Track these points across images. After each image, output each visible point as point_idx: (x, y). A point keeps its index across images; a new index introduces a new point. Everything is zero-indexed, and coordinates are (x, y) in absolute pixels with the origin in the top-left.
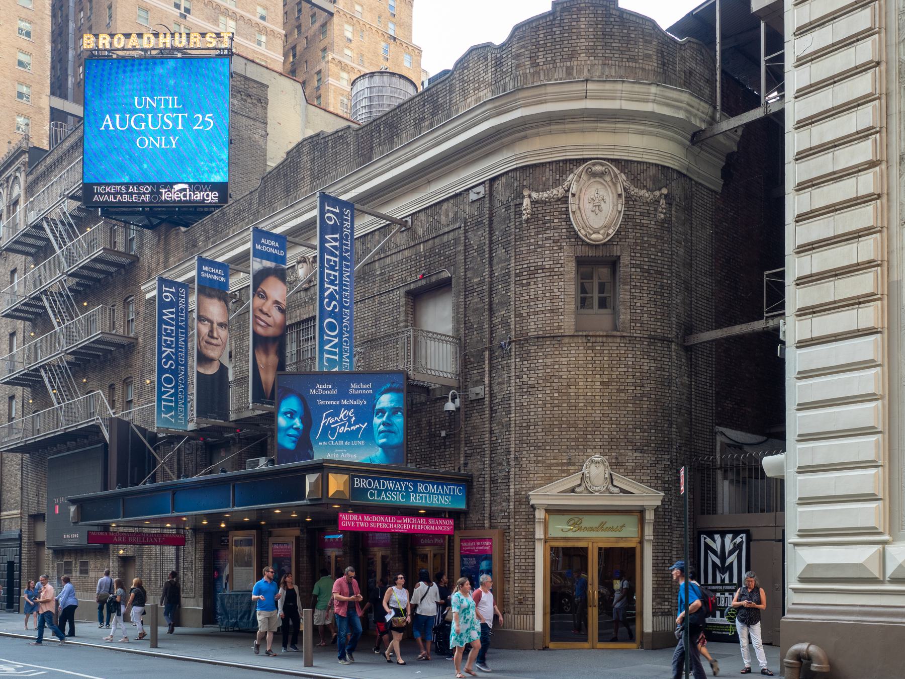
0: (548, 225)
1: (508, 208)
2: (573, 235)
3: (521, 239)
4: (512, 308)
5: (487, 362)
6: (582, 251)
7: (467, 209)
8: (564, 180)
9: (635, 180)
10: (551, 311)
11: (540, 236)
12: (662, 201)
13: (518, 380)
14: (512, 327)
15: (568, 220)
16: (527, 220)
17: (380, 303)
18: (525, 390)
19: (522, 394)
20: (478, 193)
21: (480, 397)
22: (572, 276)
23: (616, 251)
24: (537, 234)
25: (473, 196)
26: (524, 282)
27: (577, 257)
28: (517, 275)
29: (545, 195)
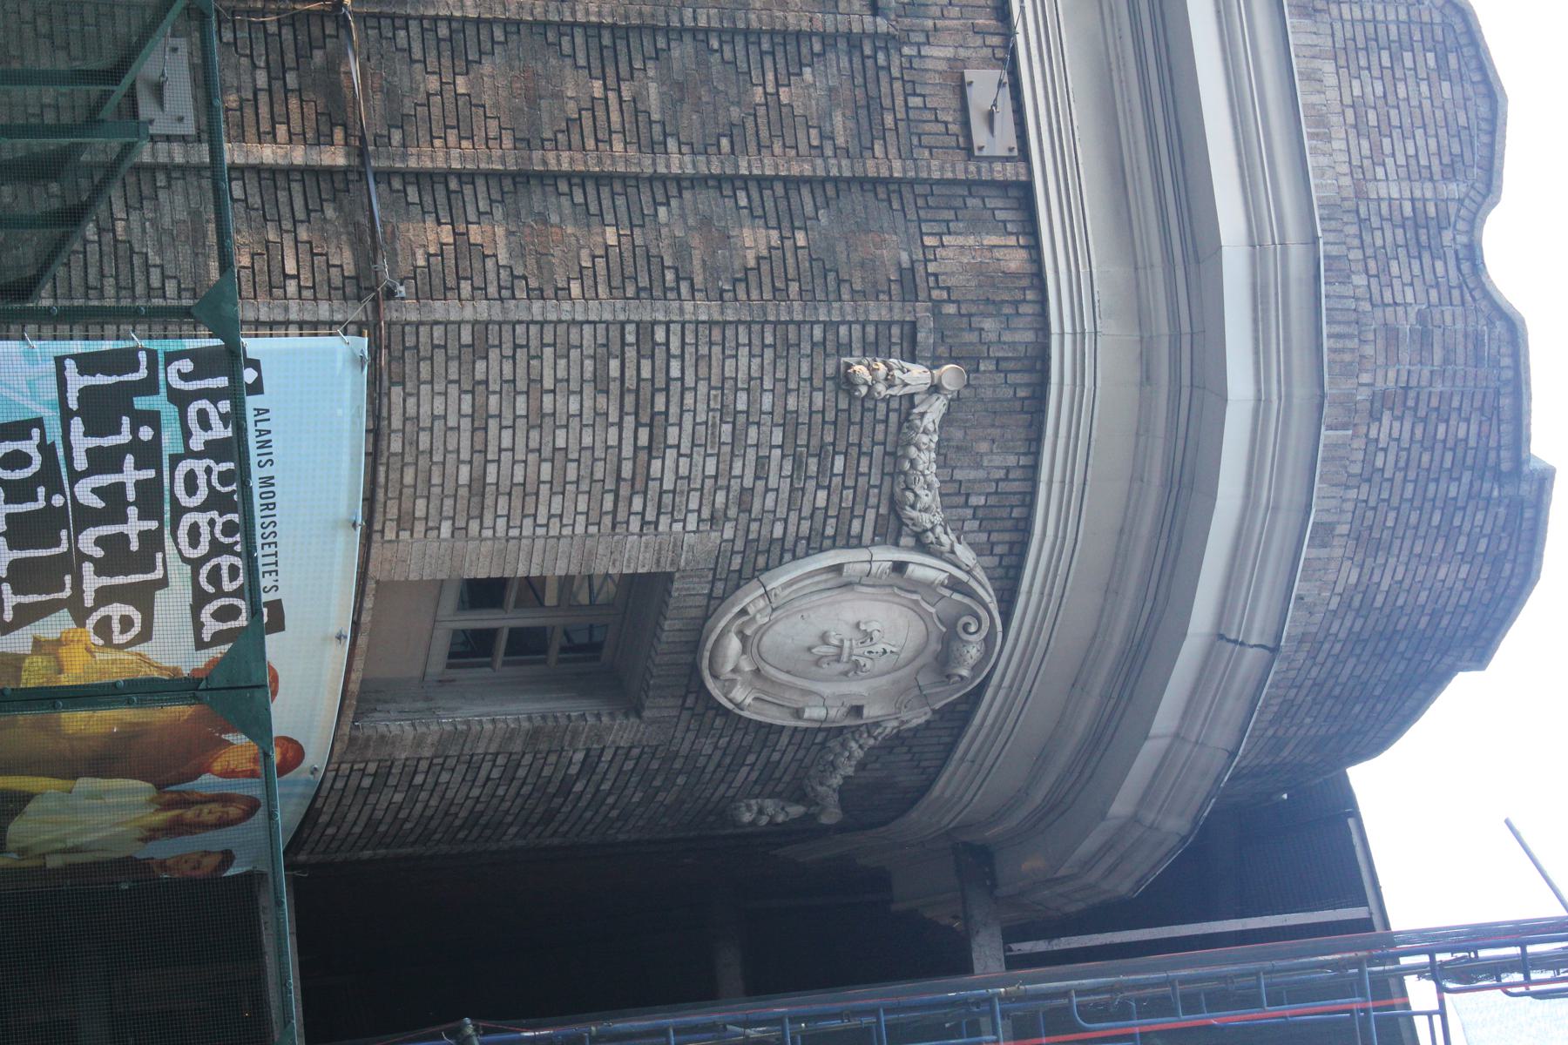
0: (813, 465)
1: (908, 283)
2: (760, 557)
3: (785, 348)
4: (516, 311)
5: (298, 156)
6: (687, 593)
7: (939, 53)
8: (960, 534)
9: (900, 739)
10: (478, 486)
11: (777, 437)
12: (796, 810)
14: (439, 310)
15: (815, 543)
16: (845, 382)
20: (990, 117)
21: (146, 109)
22: (600, 567)
23: (659, 708)
24: (789, 423)
25: (984, 85)
26: (614, 364)
27: (669, 577)
28: (645, 329)
29: (925, 459)
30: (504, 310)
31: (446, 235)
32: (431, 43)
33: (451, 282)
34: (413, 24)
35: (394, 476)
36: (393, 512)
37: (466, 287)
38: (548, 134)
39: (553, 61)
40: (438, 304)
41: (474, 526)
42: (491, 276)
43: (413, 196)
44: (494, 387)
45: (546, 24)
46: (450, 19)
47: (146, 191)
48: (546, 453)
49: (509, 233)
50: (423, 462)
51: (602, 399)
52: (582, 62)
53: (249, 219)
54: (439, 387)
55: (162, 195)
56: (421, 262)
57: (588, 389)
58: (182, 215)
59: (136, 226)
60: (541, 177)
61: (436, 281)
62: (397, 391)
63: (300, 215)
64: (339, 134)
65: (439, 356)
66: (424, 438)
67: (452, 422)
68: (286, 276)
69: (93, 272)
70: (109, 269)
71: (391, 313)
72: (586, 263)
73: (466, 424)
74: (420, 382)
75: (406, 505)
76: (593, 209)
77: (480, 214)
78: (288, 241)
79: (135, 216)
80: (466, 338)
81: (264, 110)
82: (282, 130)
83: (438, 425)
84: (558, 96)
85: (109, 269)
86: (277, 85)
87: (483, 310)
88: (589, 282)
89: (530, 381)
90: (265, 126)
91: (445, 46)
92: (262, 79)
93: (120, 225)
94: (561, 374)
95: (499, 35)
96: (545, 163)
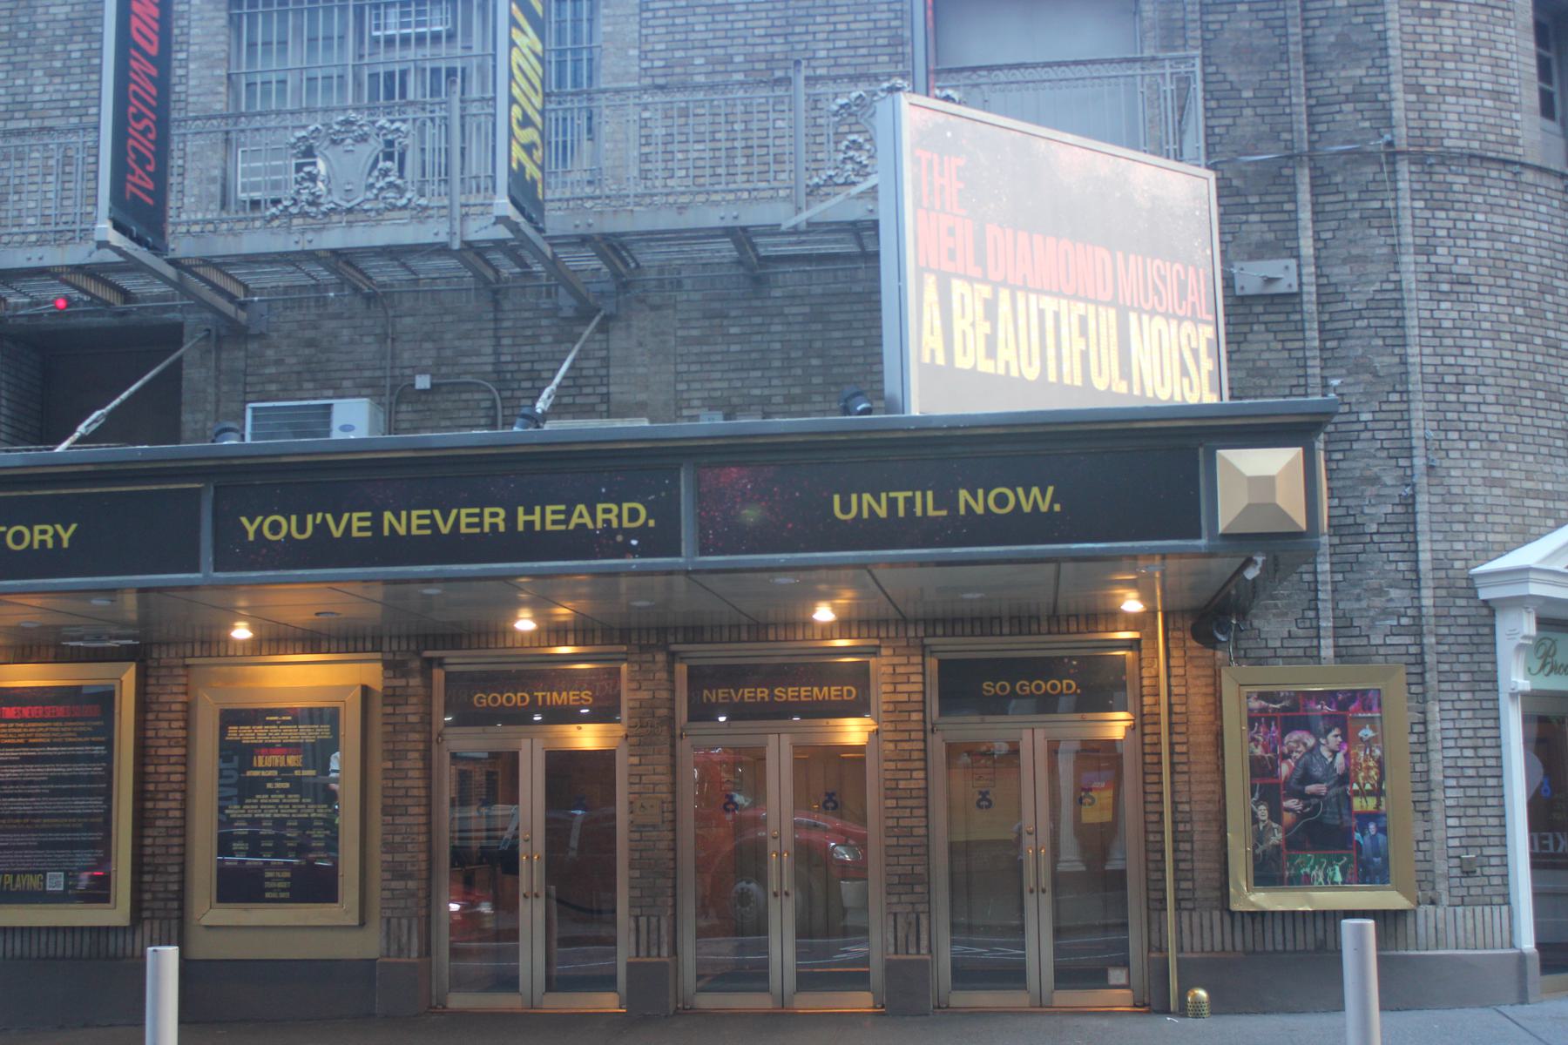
5: (1304, 195)
13: (1423, 259)
14: (1398, 114)
18: (1445, 287)
19: (1437, 296)
21: (1281, 288)
30: (1397, 73)
31: (1348, 107)
32: (1222, 112)
33: (1379, 106)
34: (1213, 122)
35: (1492, 146)
36: (1509, 148)
37: (1382, 97)
38: (1276, 41)
39: (1227, 35)
40: (1395, 114)
41: (1515, 98)
42: (1374, 80)
43: (1321, 127)
44: (1440, 81)
45: (1203, 39)
46: (1205, 100)
47: (1331, 289)
48: (1474, 50)
49: (1344, 67)
50: (1484, 128)
51: (1446, 14)
52: (1225, 17)
53: (1346, 229)
54: (1442, 116)
55: (1333, 280)
56: (1367, 124)
57: (1439, 22)
58: (1347, 269)
59: (1356, 296)
60: (1306, 46)
61: (1381, 114)
62: (1447, 142)
63: (1341, 197)
64: (1286, 172)
65: (1425, 115)
66: (1472, 127)
67: (1461, 109)
68: (1382, 208)
69: (1387, 323)
70: (1386, 313)
71: (1402, 144)
72: (1360, 19)
73: (1462, 100)
74: (1441, 128)
75: (1506, 140)
76: (1323, 13)
77: (1332, 86)
78: (1358, 205)
79: (1348, 297)
80: (1413, 98)
81: (1275, 217)
82: (1287, 207)
83: (1464, 117)
84: (1249, 33)
85: (1386, 313)
86: (1257, 208)
87: (1397, 86)
88: (1373, 18)
89: (1436, 59)
90: (1286, 217)
91: (1223, 103)
92: (1254, 218)
93: (1356, 306)
94: (1430, 38)
95: (1212, 69)
96: (1297, 43)
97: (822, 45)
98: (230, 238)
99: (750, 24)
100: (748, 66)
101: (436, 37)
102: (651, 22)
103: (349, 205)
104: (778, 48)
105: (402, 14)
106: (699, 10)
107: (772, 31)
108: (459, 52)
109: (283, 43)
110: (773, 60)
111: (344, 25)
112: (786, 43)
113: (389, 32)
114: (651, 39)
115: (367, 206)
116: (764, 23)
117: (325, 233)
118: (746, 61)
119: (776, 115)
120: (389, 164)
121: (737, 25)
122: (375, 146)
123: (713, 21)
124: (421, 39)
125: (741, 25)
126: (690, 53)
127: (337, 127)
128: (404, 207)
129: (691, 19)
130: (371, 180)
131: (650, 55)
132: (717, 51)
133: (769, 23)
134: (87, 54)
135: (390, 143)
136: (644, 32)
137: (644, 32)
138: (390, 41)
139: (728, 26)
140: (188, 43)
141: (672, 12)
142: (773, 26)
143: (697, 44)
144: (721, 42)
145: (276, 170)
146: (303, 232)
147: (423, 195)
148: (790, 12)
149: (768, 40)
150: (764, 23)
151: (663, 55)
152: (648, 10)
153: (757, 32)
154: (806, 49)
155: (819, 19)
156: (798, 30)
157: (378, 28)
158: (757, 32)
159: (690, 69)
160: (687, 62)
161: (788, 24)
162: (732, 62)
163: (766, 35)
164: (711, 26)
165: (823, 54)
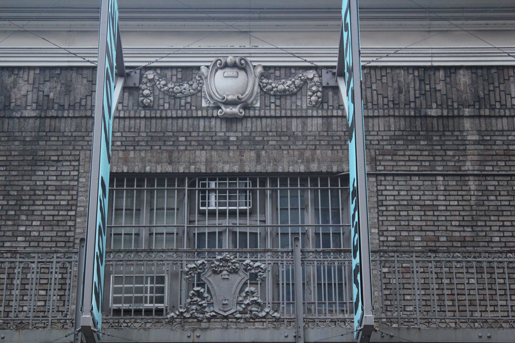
17: (484, 191)
97: (496, 234)
98: (142, 331)
99: (448, 218)
100: (449, 244)
101: (243, 213)
102: (385, 213)
103: (225, 314)
104: (468, 233)
105: (220, 197)
106: (416, 208)
107: (463, 223)
108: (258, 224)
109: (138, 210)
110: (465, 241)
111: (181, 202)
112: (473, 231)
113: (210, 208)
114: (386, 223)
115: (238, 315)
116: (458, 218)
117: (209, 332)
118: (447, 241)
119: (469, 276)
120: (253, 289)
121: (440, 218)
122: (242, 277)
123: (425, 215)
124: (233, 213)
125: (443, 218)
126: (411, 234)
127: (217, 263)
128: (264, 317)
129: (411, 213)
130: (240, 299)
131: (385, 233)
132: (428, 233)
133: (461, 218)
134: (6, 208)
135: (256, 275)
136: (381, 218)
137: (381, 218)
138: (212, 213)
139: (435, 218)
140: (76, 205)
141: (398, 208)
142: (463, 220)
143: (415, 228)
144: (432, 228)
145: (139, 290)
146: (194, 330)
147: (276, 311)
148: (474, 213)
149: (461, 229)
150: (458, 218)
151: (394, 233)
152: (382, 205)
153: (453, 223)
154: (486, 236)
155: (492, 218)
156: (479, 223)
157: (204, 205)
158: (453, 223)
159: (412, 244)
160: (410, 239)
161: (473, 220)
162: (439, 241)
163: (459, 226)
164: (423, 218)
165: (497, 239)
